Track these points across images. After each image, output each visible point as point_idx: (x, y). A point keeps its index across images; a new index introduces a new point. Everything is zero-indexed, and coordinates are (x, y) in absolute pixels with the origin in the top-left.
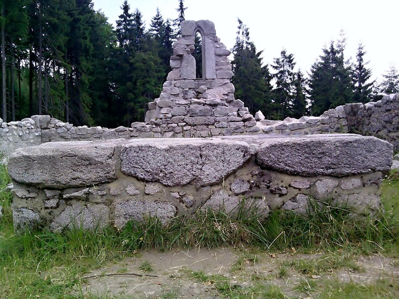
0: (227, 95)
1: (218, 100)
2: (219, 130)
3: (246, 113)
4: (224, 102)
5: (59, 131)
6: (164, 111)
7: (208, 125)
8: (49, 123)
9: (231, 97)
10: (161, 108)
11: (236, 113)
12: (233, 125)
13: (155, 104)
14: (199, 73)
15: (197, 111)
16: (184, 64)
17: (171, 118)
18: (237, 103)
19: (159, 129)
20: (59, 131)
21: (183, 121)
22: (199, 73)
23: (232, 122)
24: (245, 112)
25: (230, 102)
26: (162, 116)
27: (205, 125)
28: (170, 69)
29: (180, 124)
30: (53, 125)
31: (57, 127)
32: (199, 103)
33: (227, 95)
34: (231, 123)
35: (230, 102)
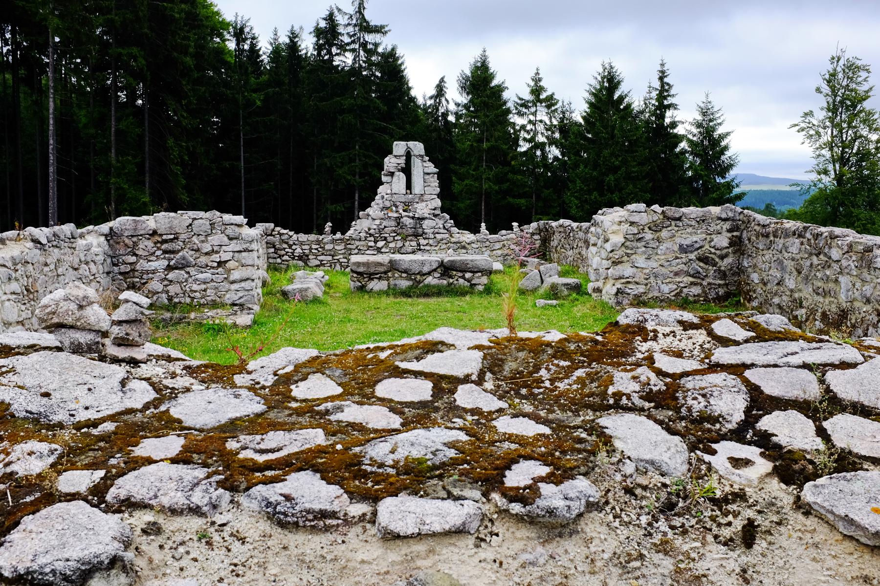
0: (434, 209)
1: (426, 215)
2: (426, 242)
3: (451, 226)
4: (431, 216)
5: (283, 238)
6: (377, 222)
7: (416, 235)
8: (273, 230)
9: (438, 212)
10: (374, 219)
11: (441, 226)
12: (439, 237)
13: (368, 215)
14: (409, 186)
15: (407, 224)
16: (395, 179)
17: (383, 229)
18: (443, 217)
19: (372, 239)
20: (283, 238)
21: (394, 232)
22: (409, 186)
23: (438, 233)
24: (450, 225)
25: (435, 216)
26: (375, 227)
27: (414, 235)
28: (382, 184)
29: (391, 235)
30: (277, 233)
31: (281, 234)
32: (409, 217)
33: (434, 209)
34: (437, 235)
35: (435, 216)
